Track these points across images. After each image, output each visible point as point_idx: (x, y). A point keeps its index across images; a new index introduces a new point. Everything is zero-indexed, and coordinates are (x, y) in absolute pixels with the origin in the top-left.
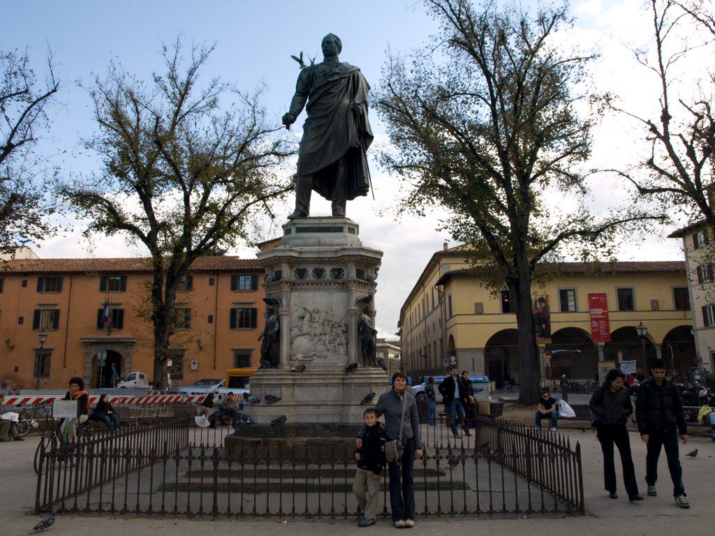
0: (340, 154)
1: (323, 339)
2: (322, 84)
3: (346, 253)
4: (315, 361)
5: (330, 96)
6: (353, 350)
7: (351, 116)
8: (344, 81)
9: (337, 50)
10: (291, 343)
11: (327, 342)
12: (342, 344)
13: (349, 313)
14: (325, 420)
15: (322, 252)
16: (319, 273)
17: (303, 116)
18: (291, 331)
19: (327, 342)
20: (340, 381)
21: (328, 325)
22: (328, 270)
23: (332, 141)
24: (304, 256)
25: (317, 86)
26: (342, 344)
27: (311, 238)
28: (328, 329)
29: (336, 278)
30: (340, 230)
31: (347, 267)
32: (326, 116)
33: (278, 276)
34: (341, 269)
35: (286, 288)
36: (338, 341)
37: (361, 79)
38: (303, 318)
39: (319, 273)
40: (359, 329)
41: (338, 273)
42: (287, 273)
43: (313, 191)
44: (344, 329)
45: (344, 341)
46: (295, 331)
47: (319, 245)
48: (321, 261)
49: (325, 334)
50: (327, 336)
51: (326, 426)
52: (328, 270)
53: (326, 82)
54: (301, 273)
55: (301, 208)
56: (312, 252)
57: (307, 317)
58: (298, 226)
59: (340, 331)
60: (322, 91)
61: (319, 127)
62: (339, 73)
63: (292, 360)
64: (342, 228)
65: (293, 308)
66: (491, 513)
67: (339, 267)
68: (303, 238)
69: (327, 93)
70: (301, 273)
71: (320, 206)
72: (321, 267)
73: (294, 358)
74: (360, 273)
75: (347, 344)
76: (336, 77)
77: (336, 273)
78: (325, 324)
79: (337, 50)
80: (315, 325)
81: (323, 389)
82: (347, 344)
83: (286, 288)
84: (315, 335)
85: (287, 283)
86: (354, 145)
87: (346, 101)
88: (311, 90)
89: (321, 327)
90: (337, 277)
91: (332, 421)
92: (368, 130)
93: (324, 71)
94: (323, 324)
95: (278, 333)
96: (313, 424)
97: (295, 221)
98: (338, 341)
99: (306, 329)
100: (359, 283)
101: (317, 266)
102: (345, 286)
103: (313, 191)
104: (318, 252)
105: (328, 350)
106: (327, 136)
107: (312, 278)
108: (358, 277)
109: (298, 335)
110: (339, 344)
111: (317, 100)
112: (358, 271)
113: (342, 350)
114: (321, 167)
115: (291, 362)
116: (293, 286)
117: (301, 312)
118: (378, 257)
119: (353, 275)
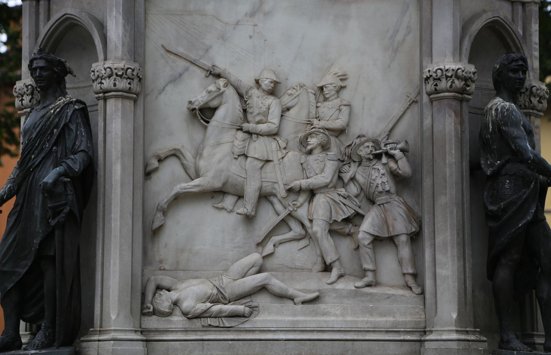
1: (302, 213)
10: (152, 233)
11: (319, 228)
12: (391, 240)
13: (433, 90)
18: (148, 174)
19: (319, 228)
21: (325, 147)
26: (391, 240)
38: (204, 114)
40: (475, 169)
45: (401, 226)
46: (170, 180)
49: (312, 193)
50: (320, 200)
57: (228, 110)
63: (155, 312)
75: (415, 238)
78: (313, 141)
80: (259, 148)
82: (415, 238)
84: (264, 197)
89: (293, 156)
94: (303, 142)
105: (327, 268)
109: (180, 199)
110: (377, 240)
115: (152, 322)
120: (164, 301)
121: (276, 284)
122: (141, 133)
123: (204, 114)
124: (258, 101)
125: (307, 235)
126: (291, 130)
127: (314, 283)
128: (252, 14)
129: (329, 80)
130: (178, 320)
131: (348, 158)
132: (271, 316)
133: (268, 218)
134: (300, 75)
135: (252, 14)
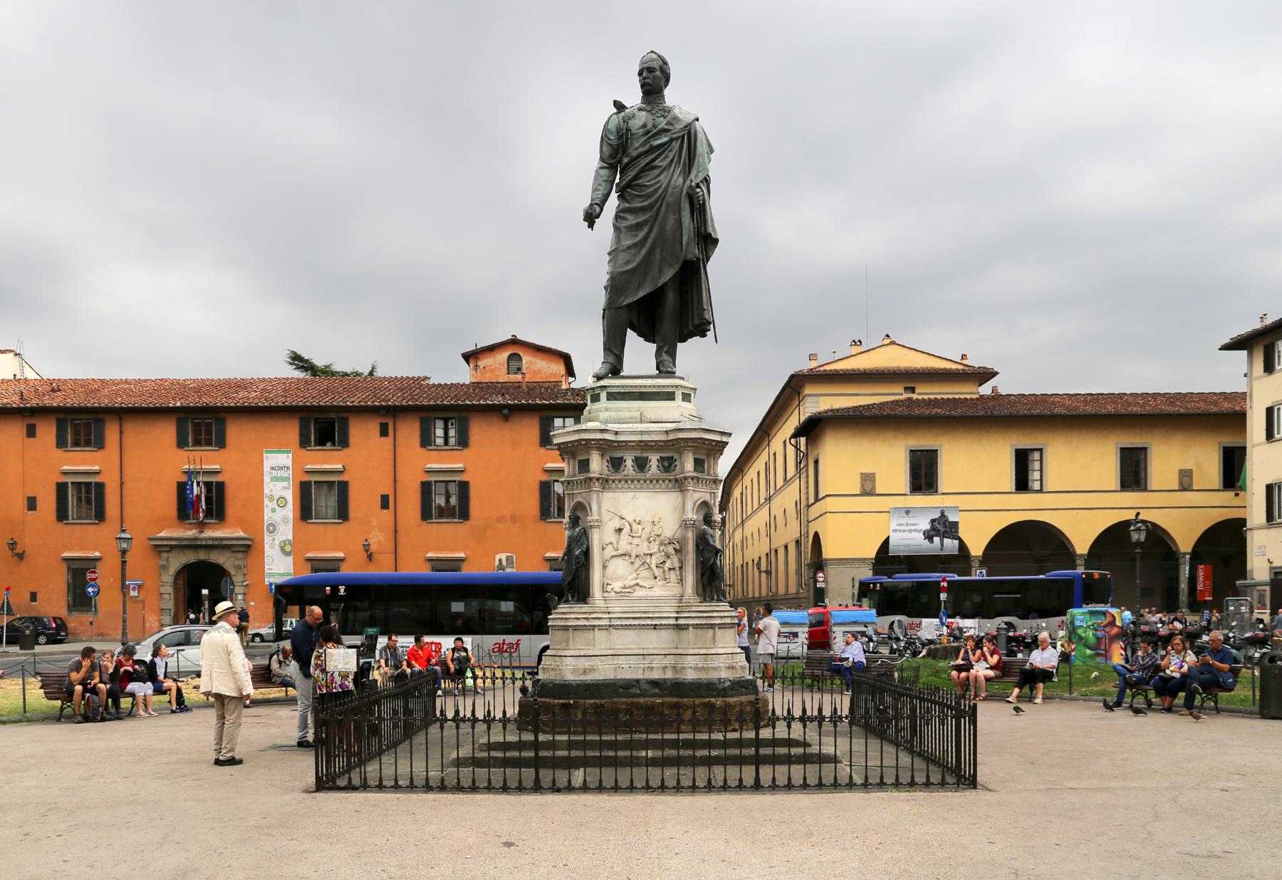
0: (668, 274)
2: (642, 150)
3: (681, 435)
4: (636, 594)
5: (657, 172)
6: (690, 578)
7: (686, 206)
8: (676, 145)
9: (663, 83)
10: (605, 567)
11: (653, 566)
13: (685, 524)
14: (655, 675)
15: (647, 432)
16: (641, 464)
17: (613, 202)
20: (672, 622)
22: (654, 459)
23: (658, 251)
24: (621, 438)
25: (634, 154)
27: (629, 410)
28: (654, 548)
30: (670, 396)
31: (680, 454)
32: (650, 207)
33: (584, 466)
35: (596, 486)
36: (668, 565)
37: (700, 135)
38: (620, 530)
39: (641, 464)
40: (697, 546)
41: (668, 464)
42: (597, 464)
43: (629, 332)
44: (678, 547)
45: (677, 565)
46: (609, 551)
47: (641, 422)
48: (646, 446)
51: (654, 683)
52: (654, 459)
53: (646, 148)
54: (617, 464)
55: (611, 359)
56: (633, 433)
58: (609, 390)
59: (670, 549)
60: (643, 163)
61: (638, 226)
62: (668, 131)
64: (673, 393)
65: (606, 516)
66: (866, 785)
68: (617, 410)
69: (649, 167)
70: (617, 464)
71: (639, 354)
73: (609, 588)
74: (699, 464)
75: (681, 568)
76: (664, 139)
77: (666, 464)
79: (663, 83)
80: (636, 541)
81: (653, 633)
83: (596, 486)
85: (598, 479)
86: (690, 257)
87: (678, 180)
88: (626, 160)
89: (646, 543)
91: (663, 677)
92: (710, 230)
93: (644, 126)
95: (587, 554)
96: (638, 681)
97: (602, 383)
98: (668, 565)
99: (624, 546)
100: (698, 479)
101: (638, 454)
102: (680, 485)
103: (629, 332)
106: (650, 241)
108: (695, 470)
111: (636, 178)
112: (696, 460)
113: (673, 576)
114: (641, 294)
116: (605, 483)
117: (617, 523)
118: (724, 439)
119: (689, 465)
120: (609, 588)
121: (641, 583)
122: (601, 538)
123: (620, 530)
124: (635, 526)
125: (649, 568)
126: (645, 536)
127: (652, 582)
129: (656, 520)
130: (613, 594)
131: (661, 544)
132: (640, 593)
133: (638, 562)
134: (647, 518)
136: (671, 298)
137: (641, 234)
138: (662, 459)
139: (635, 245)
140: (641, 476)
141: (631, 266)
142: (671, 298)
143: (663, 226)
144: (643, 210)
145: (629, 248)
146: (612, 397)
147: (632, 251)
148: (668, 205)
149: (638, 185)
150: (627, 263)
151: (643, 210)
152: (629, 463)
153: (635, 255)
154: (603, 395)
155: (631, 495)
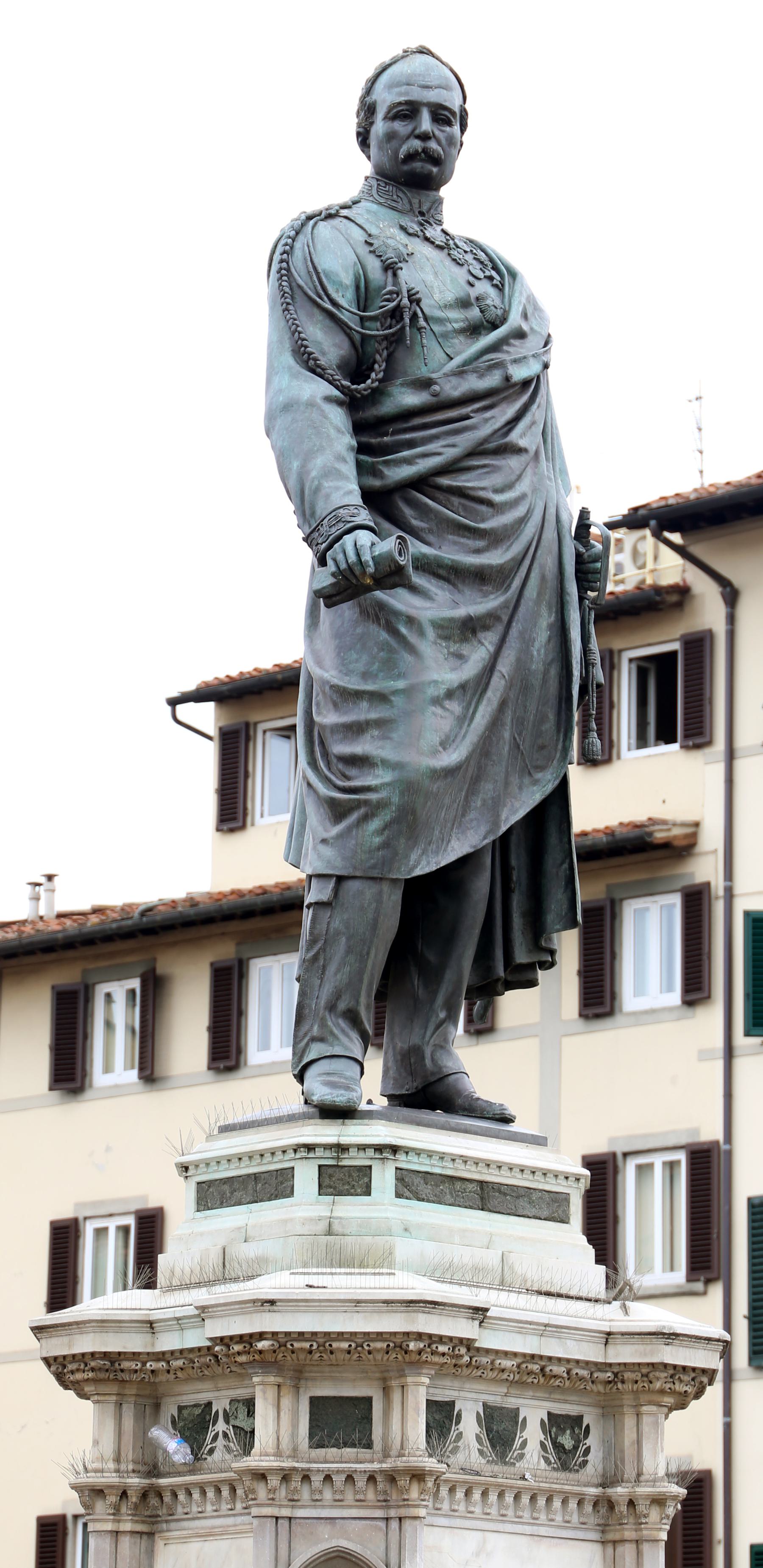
5: (513, 462)
16: (500, 1430)
23: (508, 718)
29: (565, 1467)
34: (579, 1419)
39: (500, 1430)
48: (535, 1372)
53: (493, 380)
56: (523, 1326)
58: (403, 1162)
61: (470, 628)
67: (571, 1409)
68: (435, 1235)
72: (511, 1402)
90: (565, 1458)
101: (496, 1396)
104: (547, 1329)
107: (476, 1460)
128: (478, 1554)
135: (478, 1554)
136: (481, 885)
137: (478, 655)
138: (555, 1423)
139: (463, 687)
140: (502, 1475)
141: (452, 757)
142: (481, 885)
143: (527, 642)
144: (481, 577)
145: (450, 694)
146: (409, 1186)
147: (455, 707)
148: (543, 578)
149: (461, 492)
150: (445, 744)
151: (481, 577)
152: (469, 1426)
153: (465, 719)
154: (384, 1177)
155: (472, 1539)
